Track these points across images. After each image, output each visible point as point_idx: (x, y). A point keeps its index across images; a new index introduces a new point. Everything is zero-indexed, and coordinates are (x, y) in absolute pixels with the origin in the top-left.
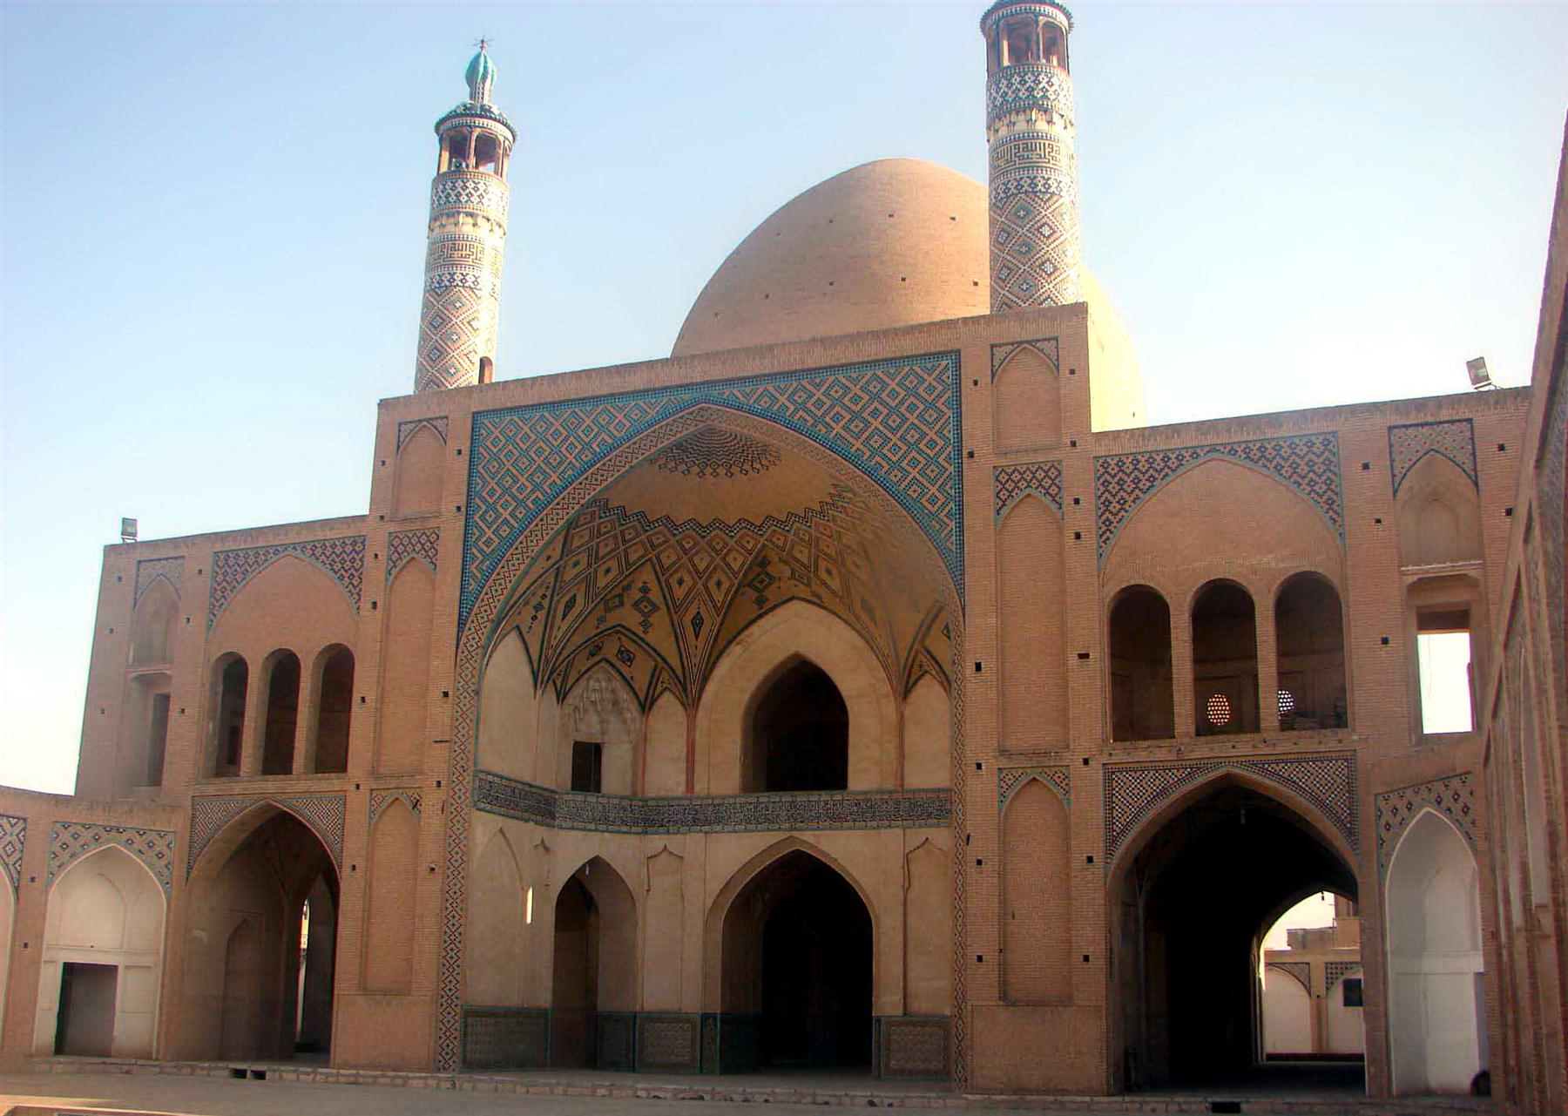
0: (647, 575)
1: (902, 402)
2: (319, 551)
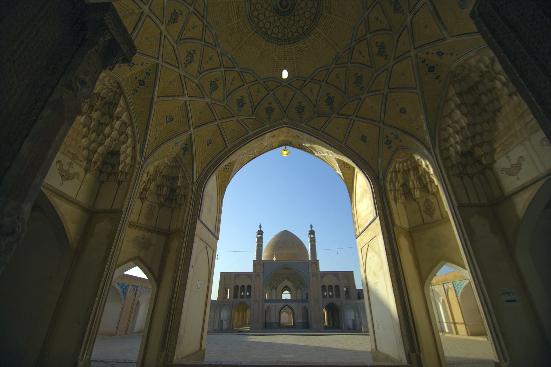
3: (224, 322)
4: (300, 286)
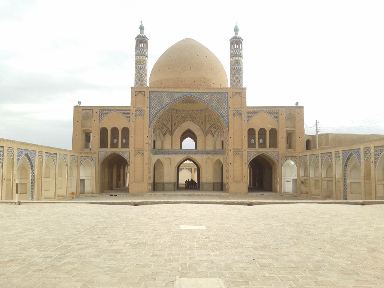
0: (170, 117)
1: (220, 99)
2: (121, 111)
3: (87, 183)
4: (212, 129)
